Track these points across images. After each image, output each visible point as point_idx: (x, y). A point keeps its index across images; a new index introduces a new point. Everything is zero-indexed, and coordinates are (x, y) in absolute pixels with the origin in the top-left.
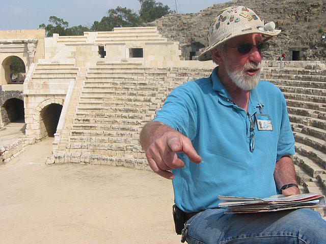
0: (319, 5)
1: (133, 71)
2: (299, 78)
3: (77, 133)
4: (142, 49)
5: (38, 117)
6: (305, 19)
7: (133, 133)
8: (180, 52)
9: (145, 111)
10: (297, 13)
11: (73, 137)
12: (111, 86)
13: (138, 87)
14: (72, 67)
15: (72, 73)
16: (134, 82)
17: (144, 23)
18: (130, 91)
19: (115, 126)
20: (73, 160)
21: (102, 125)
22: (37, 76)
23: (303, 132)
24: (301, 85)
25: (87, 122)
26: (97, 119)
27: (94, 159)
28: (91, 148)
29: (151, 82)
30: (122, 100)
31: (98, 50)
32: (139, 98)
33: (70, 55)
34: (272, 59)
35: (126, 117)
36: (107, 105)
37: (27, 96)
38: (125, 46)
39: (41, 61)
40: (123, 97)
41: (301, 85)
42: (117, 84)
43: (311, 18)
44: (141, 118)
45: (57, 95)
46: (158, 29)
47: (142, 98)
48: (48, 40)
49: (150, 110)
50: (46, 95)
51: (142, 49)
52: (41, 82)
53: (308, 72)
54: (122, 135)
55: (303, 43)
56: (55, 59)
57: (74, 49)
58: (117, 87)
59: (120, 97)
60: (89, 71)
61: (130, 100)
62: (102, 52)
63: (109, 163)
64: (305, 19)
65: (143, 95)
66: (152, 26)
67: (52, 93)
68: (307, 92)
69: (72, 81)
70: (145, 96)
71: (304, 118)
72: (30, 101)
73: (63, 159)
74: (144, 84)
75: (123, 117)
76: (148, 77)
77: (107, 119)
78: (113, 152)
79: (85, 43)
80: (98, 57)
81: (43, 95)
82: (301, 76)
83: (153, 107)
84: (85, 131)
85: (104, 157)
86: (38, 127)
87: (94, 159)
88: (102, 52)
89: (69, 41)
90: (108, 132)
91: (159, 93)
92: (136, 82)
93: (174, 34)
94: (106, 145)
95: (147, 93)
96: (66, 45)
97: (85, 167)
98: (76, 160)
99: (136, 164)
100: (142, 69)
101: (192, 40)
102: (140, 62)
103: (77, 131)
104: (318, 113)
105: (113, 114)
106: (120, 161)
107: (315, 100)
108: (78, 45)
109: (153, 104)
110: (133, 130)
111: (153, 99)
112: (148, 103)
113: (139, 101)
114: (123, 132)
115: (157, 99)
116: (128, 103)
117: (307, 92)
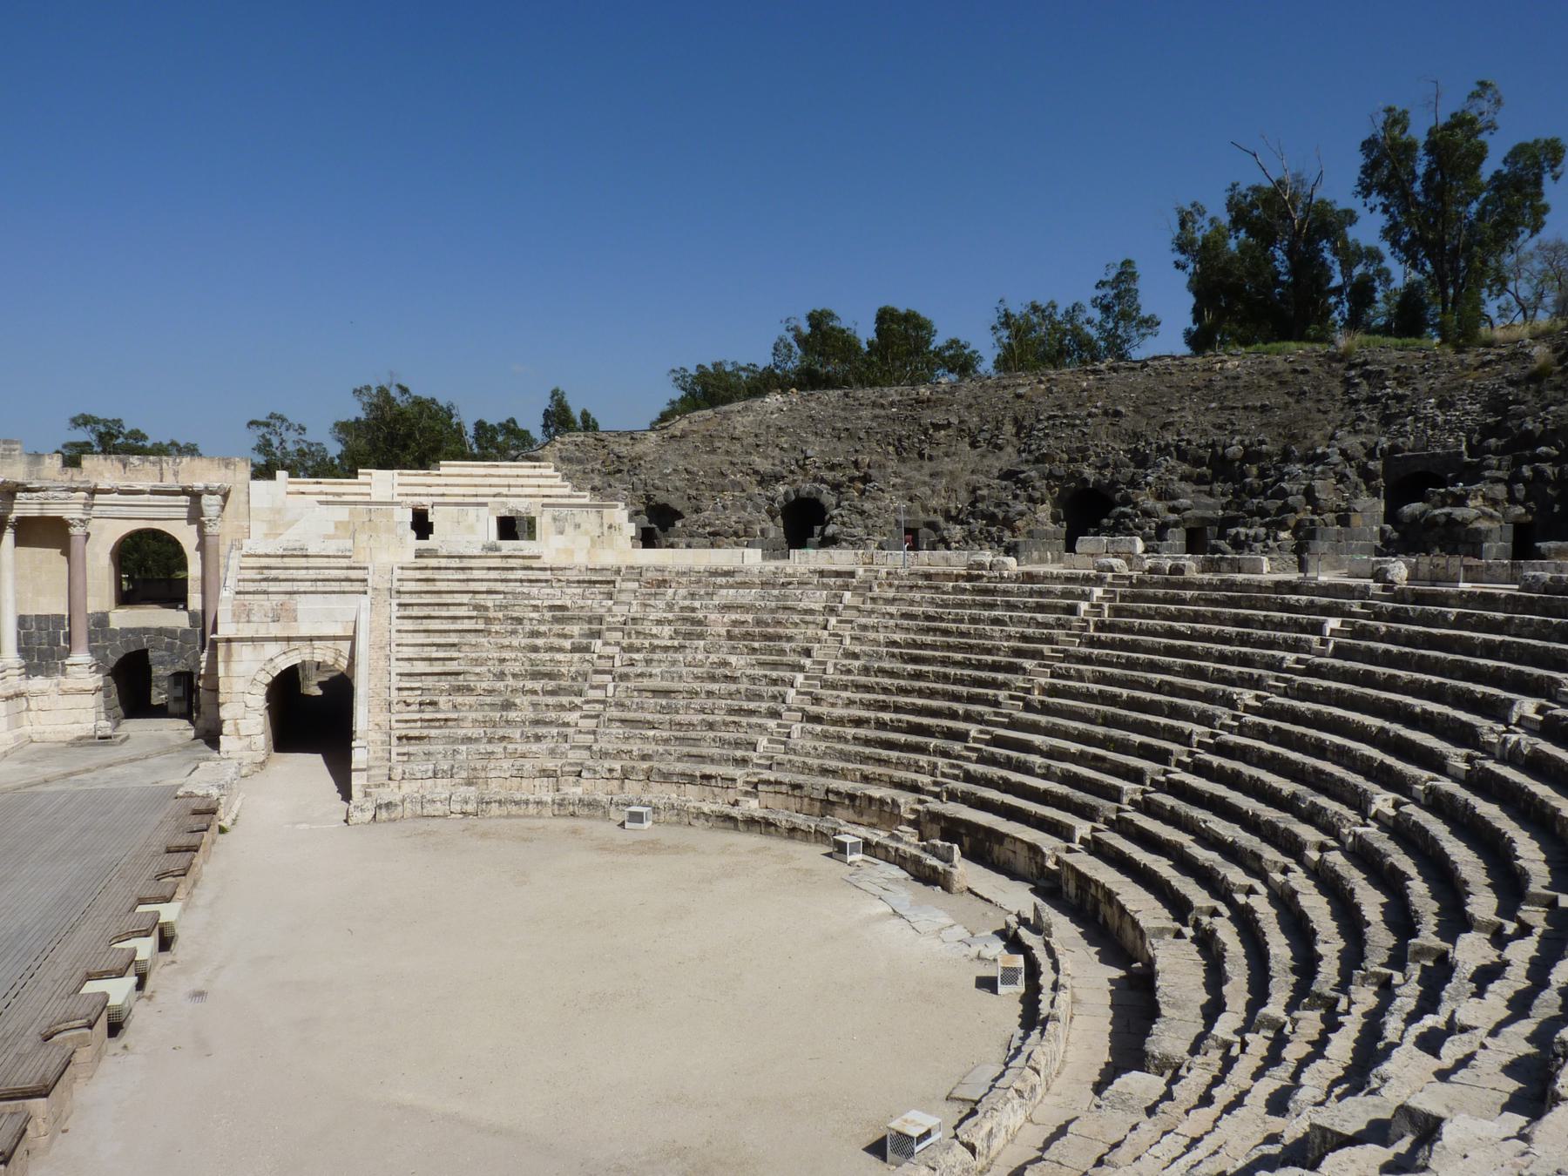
0: (949, 425)
1: (520, 574)
2: (963, 591)
3: (409, 738)
4: (534, 519)
5: (258, 700)
6: (921, 456)
7: (570, 731)
8: (631, 529)
9: (585, 676)
10: (900, 440)
11: (405, 750)
12: (474, 613)
13: (548, 615)
14: (344, 562)
15: (352, 581)
17: (513, 452)
18: (528, 628)
19: (512, 715)
20: (429, 809)
21: (479, 716)
22: (251, 587)
23: (1028, 707)
24: (974, 604)
25: (430, 708)
26: (459, 699)
28: (464, 774)
29: (581, 603)
31: (410, 519)
32: (557, 642)
33: (331, 531)
34: (866, 547)
35: (534, 692)
36: (477, 662)
37: (229, 640)
38: (485, 509)
39: (248, 546)
41: (974, 604)
42: (486, 608)
43: (934, 453)
44: (580, 693)
45: (320, 638)
46: (557, 470)
47: (567, 644)
48: (261, 485)
49: (597, 672)
50: (289, 639)
51: (534, 519)
52: (267, 603)
53: (981, 577)
54: (538, 738)
55: (925, 509)
56: (289, 538)
57: (342, 513)
58: (491, 614)
59: (506, 642)
60: (398, 573)
61: (535, 649)
62: (422, 525)
63: (532, 809)
64: (921, 456)
65: (565, 636)
66: (537, 459)
67: (305, 631)
68: (996, 621)
69: (365, 601)
71: (1018, 680)
72: (235, 658)
74: (563, 608)
75: (525, 692)
76: (568, 591)
77: (488, 700)
79: (367, 499)
80: (412, 541)
81: (276, 639)
82: (968, 585)
83: (604, 664)
84: (433, 733)
85: (518, 797)
86: (260, 729)
88: (422, 525)
89: (321, 493)
90: (501, 732)
91: (609, 629)
92: (538, 603)
93: (597, 481)
94: (506, 764)
95: (575, 629)
96: (321, 503)
97: (465, 822)
98: (440, 808)
99: (613, 809)
100: (545, 569)
101: (648, 498)
102: (536, 553)
103: (412, 733)
104: (1045, 666)
105: (500, 685)
107: (1024, 638)
108: (355, 503)
109: (600, 657)
111: (597, 644)
112: (588, 656)
113: (560, 650)
114: (541, 731)
115: (606, 644)
116: (533, 656)
117: (996, 621)
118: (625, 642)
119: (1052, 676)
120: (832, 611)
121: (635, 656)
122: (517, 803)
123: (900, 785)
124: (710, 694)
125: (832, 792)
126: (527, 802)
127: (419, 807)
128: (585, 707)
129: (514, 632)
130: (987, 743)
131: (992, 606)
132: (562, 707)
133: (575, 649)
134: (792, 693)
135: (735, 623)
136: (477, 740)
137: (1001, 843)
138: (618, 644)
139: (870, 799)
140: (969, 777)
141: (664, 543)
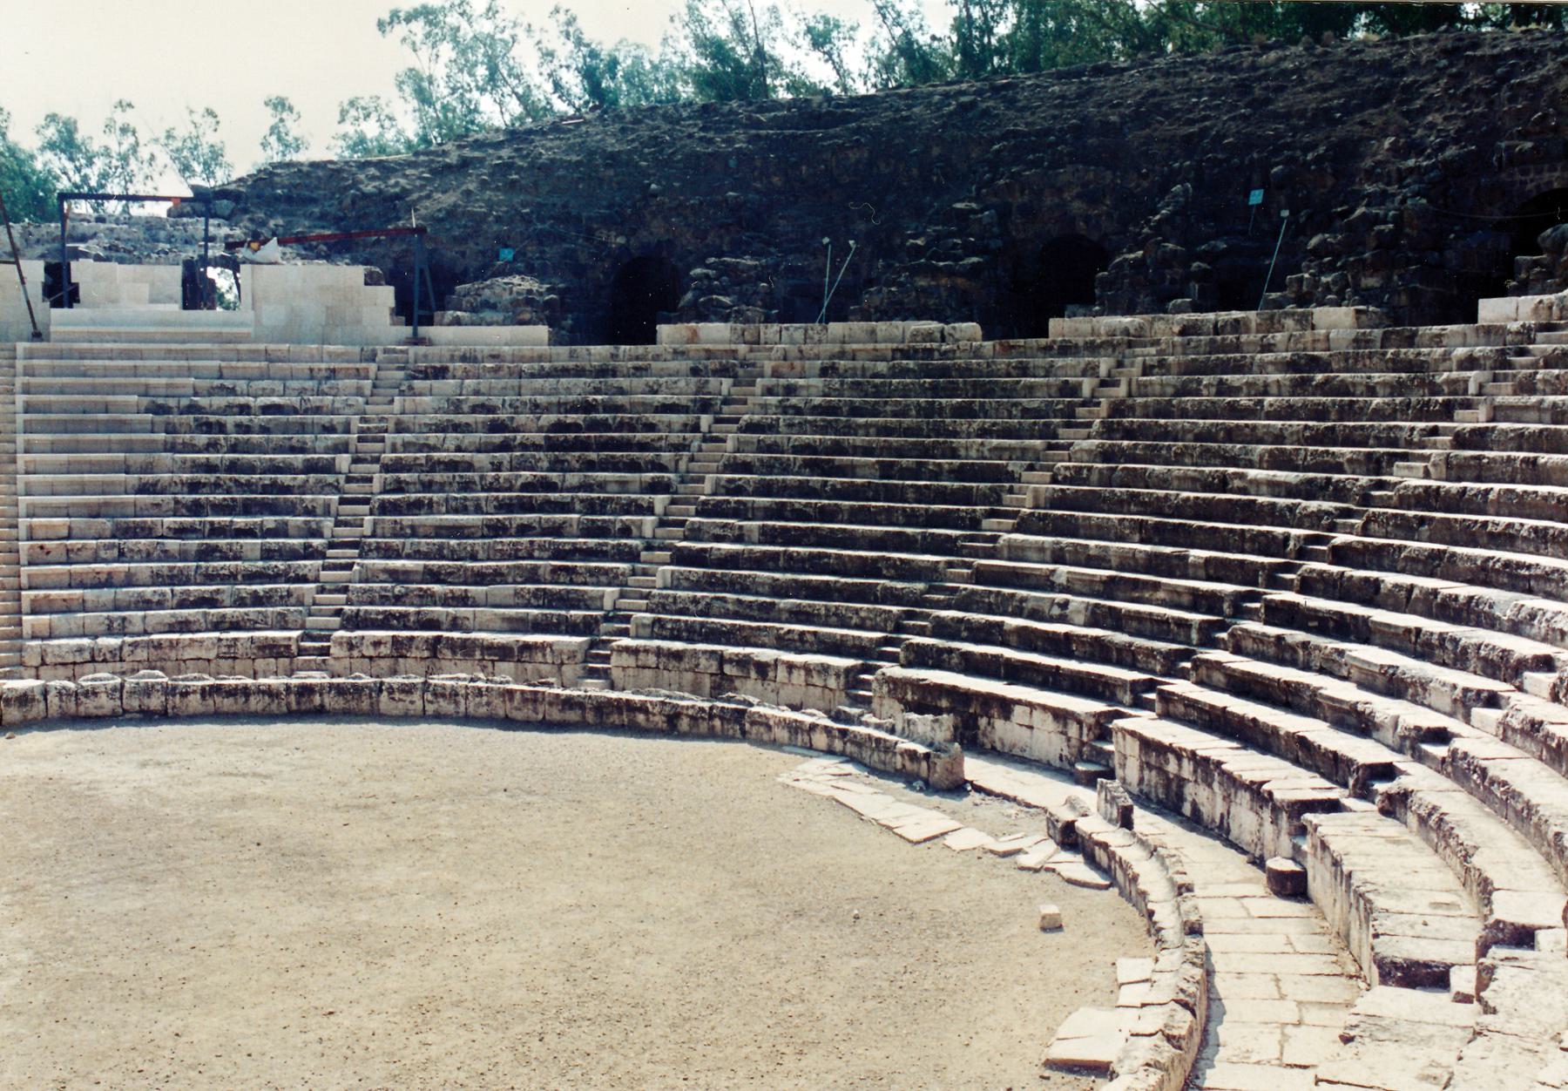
16: (242, 400)
20: (89, 706)
27: (184, 694)
28: (142, 654)
30: (209, 468)
40: (214, 457)
44: (317, 533)
47: (298, 459)
49: (343, 502)
54: (257, 600)
58: (175, 418)
65: (293, 450)
70: (302, 450)
73: (42, 706)
78: (239, 665)
87: (184, 694)
98: (106, 704)
106: (306, 691)
109: (349, 480)
110: (303, 579)
111: (343, 461)
112: (330, 478)
117: (959, 412)
118: (388, 457)
119: (1054, 481)
120: (705, 407)
121: (404, 476)
122: (232, 692)
123: (837, 648)
124: (524, 530)
125: (730, 661)
126: (246, 691)
127: (72, 705)
128: (330, 552)
129: (212, 446)
130: (968, 580)
131: (952, 392)
132: (294, 554)
133: (310, 468)
134: (649, 520)
135: (559, 427)
136: (160, 605)
137: (1007, 716)
138: (376, 460)
139: (791, 667)
140: (942, 629)
141: (438, 315)
